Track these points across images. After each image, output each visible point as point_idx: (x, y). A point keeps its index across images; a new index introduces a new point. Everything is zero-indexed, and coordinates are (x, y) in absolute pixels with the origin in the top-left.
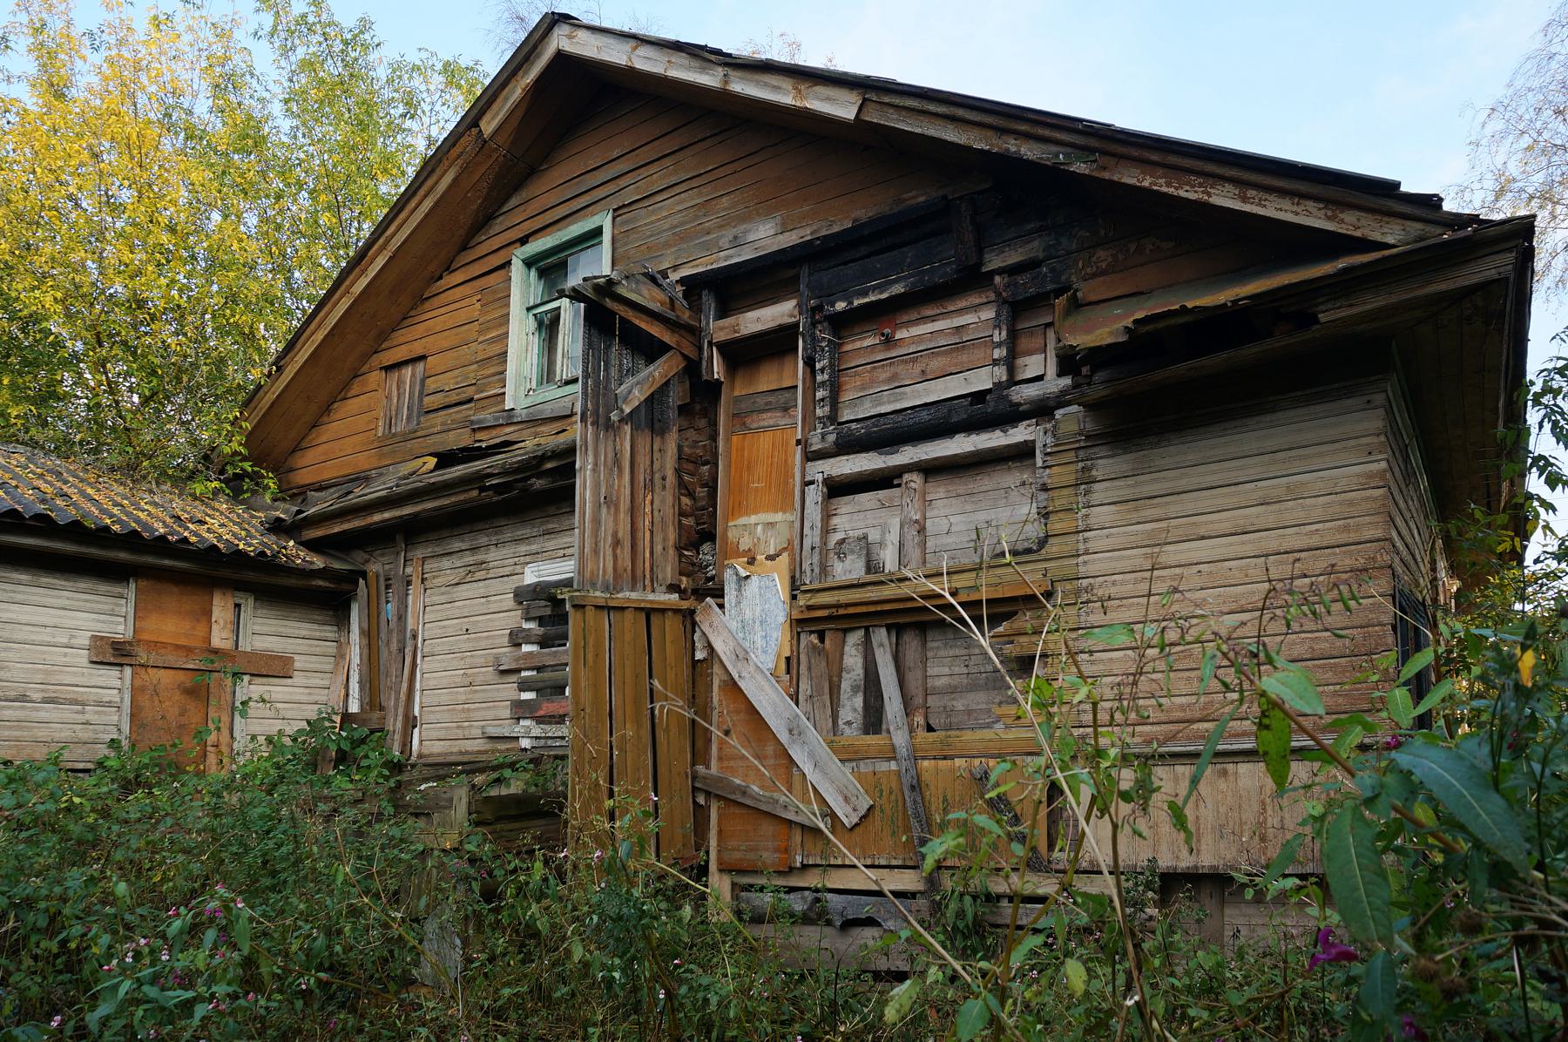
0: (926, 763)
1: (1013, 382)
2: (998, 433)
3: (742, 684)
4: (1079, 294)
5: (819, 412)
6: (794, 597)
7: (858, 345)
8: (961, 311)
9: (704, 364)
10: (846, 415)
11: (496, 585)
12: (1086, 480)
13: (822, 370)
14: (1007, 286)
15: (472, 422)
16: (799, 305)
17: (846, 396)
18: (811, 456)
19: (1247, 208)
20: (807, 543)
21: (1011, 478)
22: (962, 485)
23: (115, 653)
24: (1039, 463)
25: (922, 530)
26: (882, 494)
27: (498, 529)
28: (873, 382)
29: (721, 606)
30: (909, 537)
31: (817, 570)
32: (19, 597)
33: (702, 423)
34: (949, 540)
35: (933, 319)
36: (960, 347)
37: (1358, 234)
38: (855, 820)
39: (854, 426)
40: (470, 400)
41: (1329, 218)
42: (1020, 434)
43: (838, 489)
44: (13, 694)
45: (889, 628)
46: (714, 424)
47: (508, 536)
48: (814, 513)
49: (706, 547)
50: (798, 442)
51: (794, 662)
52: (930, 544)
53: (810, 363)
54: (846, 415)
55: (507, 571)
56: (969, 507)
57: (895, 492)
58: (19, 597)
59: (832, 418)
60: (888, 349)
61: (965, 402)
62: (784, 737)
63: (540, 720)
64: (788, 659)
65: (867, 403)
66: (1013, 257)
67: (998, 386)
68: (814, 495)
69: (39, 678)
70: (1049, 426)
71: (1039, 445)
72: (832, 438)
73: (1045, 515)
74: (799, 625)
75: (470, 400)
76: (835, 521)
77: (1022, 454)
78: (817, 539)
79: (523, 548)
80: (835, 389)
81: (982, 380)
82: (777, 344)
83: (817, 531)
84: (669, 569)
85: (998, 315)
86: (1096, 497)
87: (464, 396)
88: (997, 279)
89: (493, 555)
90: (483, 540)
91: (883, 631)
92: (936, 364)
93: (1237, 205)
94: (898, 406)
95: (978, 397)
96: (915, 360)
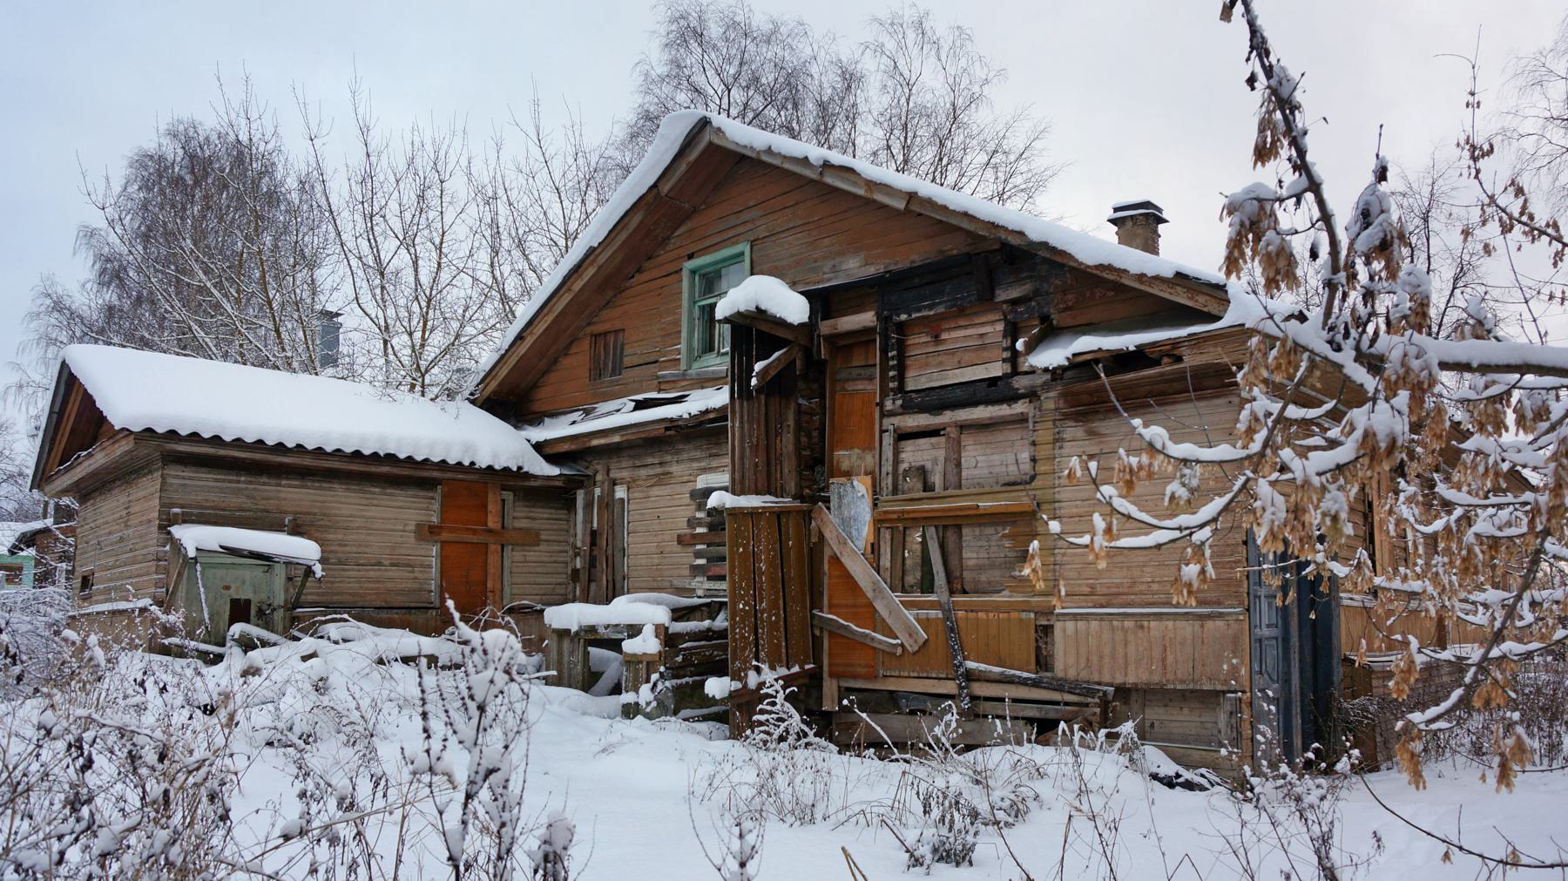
0: (961, 614)
1: (1015, 372)
2: (1005, 406)
3: (843, 560)
4: (1055, 322)
5: (891, 385)
6: (875, 505)
7: (916, 341)
8: (983, 324)
9: (815, 349)
10: (911, 385)
11: (678, 488)
12: (1058, 440)
13: (893, 358)
14: (1011, 312)
15: (658, 377)
16: (877, 314)
17: (910, 374)
18: (883, 415)
20: (884, 470)
21: (1014, 435)
22: (983, 437)
23: (427, 532)
24: (1031, 427)
25: (959, 465)
26: (934, 440)
27: (678, 452)
28: (927, 365)
29: (828, 508)
30: (949, 469)
31: (890, 488)
32: (375, 502)
33: (815, 386)
34: (976, 472)
35: (965, 327)
36: (983, 347)
37: (1206, 309)
38: (916, 648)
39: (914, 395)
40: (656, 362)
41: (1189, 298)
42: (1020, 407)
43: (903, 436)
44: (373, 561)
46: (823, 387)
48: (888, 452)
49: (818, 468)
50: (877, 404)
51: (876, 547)
52: (964, 474)
53: (884, 351)
54: (911, 385)
55: (685, 479)
56: (989, 451)
57: (943, 439)
58: (375, 502)
59: (901, 389)
60: (937, 345)
61: (984, 385)
62: (870, 595)
63: (710, 578)
64: (872, 544)
65: (923, 379)
66: (1015, 293)
67: (1006, 376)
68: (888, 440)
69: (388, 551)
70: (1037, 404)
71: (1031, 415)
72: (899, 402)
73: (1034, 460)
74: (879, 522)
75: (656, 362)
76: (903, 456)
77: (1022, 420)
78: (890, 469)
79: (695, 465)
80: (902, 369)
81: (997, 370)
82: (862, 337)
83: (891, 462)
84: (793, 485)
85: (1005, 331)
87: (653, 359)
88: (1005, 306)
89: (675, 469)
90: (668, 458)
91: (933, 529)
92: (967, 357)
94: (944, 383)
95: (993, 381)
96: (953, 354)
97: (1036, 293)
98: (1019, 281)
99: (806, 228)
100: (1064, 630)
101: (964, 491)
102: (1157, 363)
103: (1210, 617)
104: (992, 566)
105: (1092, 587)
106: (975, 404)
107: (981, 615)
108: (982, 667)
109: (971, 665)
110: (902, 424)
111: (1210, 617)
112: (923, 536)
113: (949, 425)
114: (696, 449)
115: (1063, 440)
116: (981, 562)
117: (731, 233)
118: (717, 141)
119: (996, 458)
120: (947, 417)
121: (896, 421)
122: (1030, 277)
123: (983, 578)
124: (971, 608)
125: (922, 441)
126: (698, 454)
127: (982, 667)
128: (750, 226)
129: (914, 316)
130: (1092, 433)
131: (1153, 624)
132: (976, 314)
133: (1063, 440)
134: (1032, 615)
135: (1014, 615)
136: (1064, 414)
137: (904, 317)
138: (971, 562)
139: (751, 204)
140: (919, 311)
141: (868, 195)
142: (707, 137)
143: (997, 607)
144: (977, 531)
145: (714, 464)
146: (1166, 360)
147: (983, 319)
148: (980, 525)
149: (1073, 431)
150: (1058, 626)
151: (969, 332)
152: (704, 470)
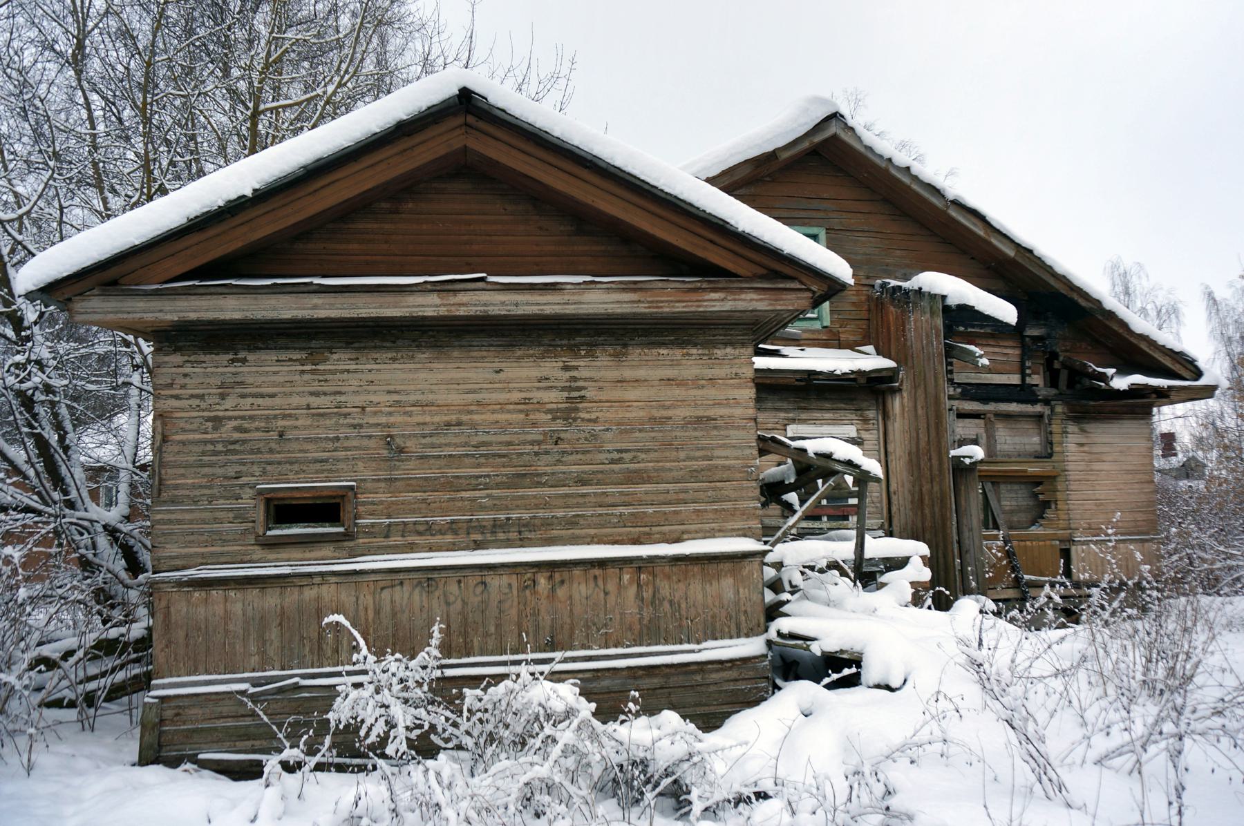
8: (1006, 347)
19: (1151, 352)
21: (1028, 426)
26: (977, 421)
34: (1006, 447)
35: (993, 346)
42: (1038, 408)
45: (992, 483)
47: (769, 405)
52: (998, 447)
55: (770, 426)
77: (1040, 417)
79: (782, 415)
86: (1069, 440)
88: (1027, 339)
91: (990, 484)
93: (1148, 350)
97: (1049, 336)
98: (1037, 326)
99: (879, 235)
100: (1077, 551)
101: (999, 459)
102: (1143, 397)
103: (1147, 541)
104: (1019, 511)
105: (1089, 524)
106: (1009, 401)
107: (1028, 543)
108: (1033, 578)
109: (1027, 577)
110: (960, 407)
111: (1147, 541)
112: (983, 489)
113: (990, 412)
114: (781, 400)
115: (1067, 433)
116: (1012, 508)
117: (802, 214)
118: (844, 136)
119: (1017, 440)
120: (991, 407)
121: (956, 403)
122: (1045, 325)
123: (1015, 519)
124: (1022, 539)
125: (967, 420)
126: (785, 405)
127: (1033, 578)
128: (820, 215)
129: (969, 330)
130: (1083, 431)
131: (1121, 545)
132: (1002, 339)
133: (1067, 433)
134: (1058, 542)
135: (1048, 543)
136: (1068, 416)
137: (962, 329)
138: (1007, 508)
139: (825, 196)
140: (973, 326)
141: (987, 237)
142: (833, 129)
143: (1037, 538)
144: (1009, 487)
145: (804, 416)
146: (1154, 396)
147: (1006, 344)
148: (1011, 483)
149: (1072, 428)
150: (1073, 548)
151: (996, 350)
152: (793, 421)
